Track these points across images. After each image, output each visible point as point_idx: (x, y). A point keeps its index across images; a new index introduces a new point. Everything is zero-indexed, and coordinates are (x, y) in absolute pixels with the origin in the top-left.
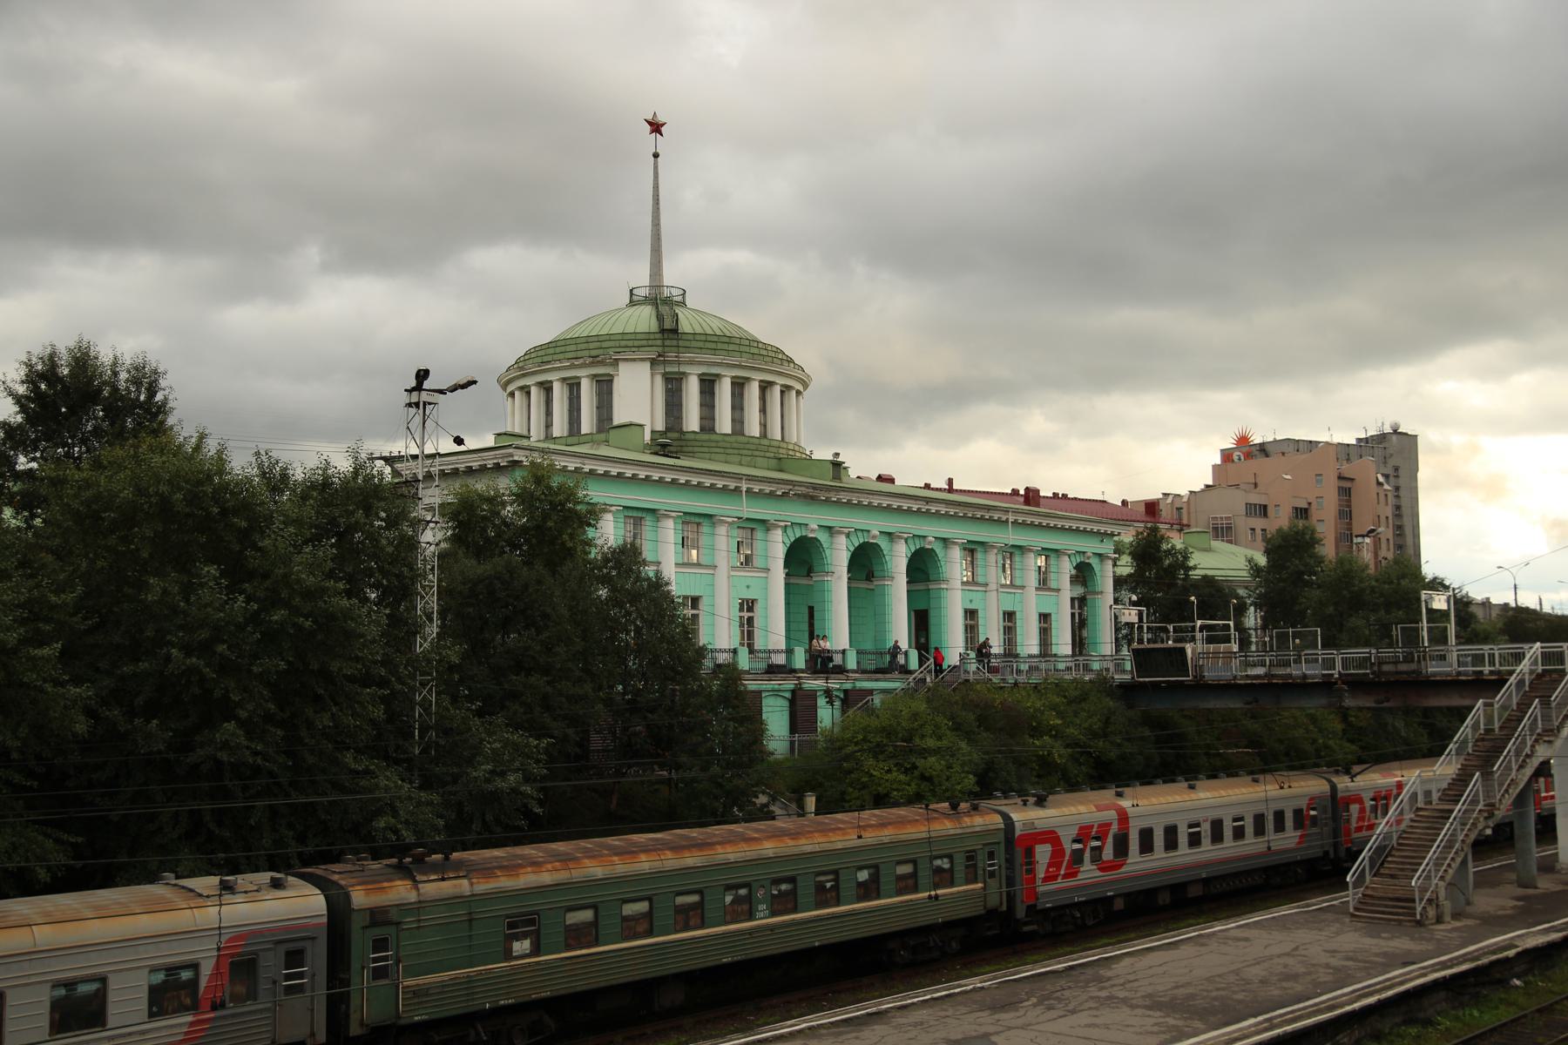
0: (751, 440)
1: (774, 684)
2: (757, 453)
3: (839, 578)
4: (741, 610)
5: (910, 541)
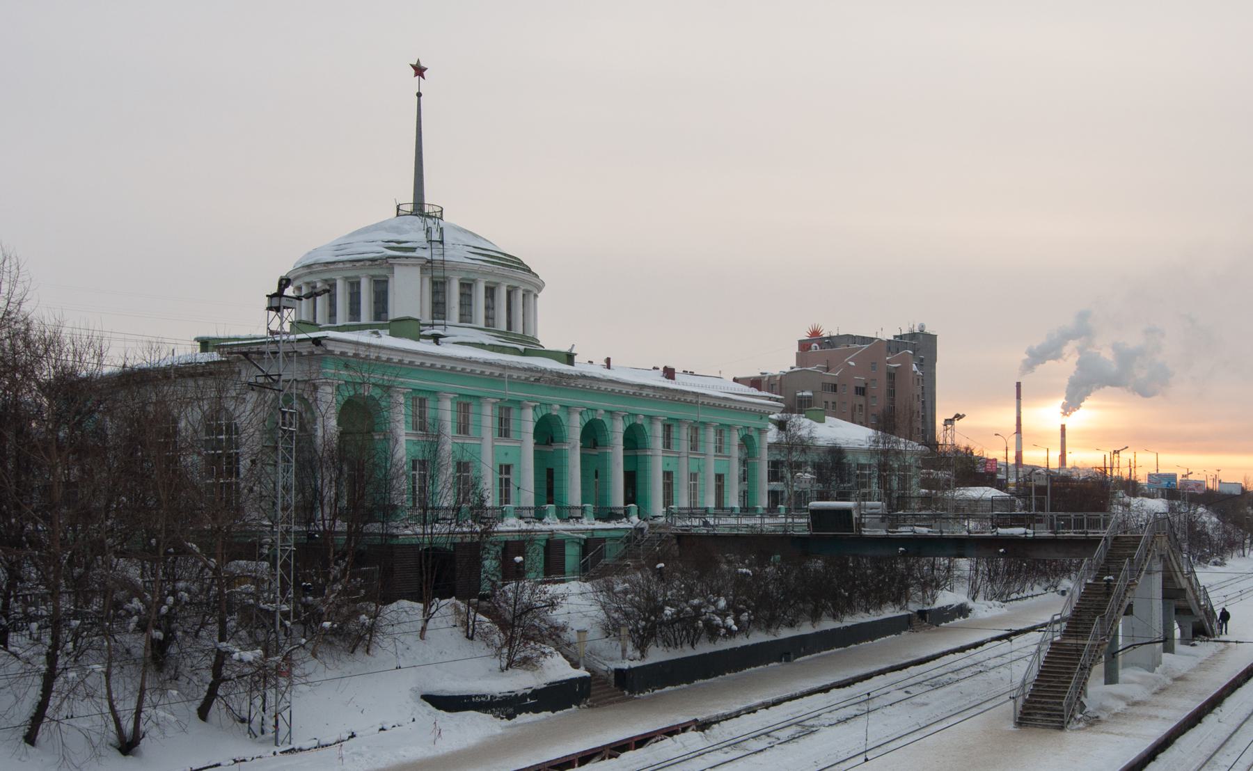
3: (574, 447)
4: (501, 473)
5: (626, 419)
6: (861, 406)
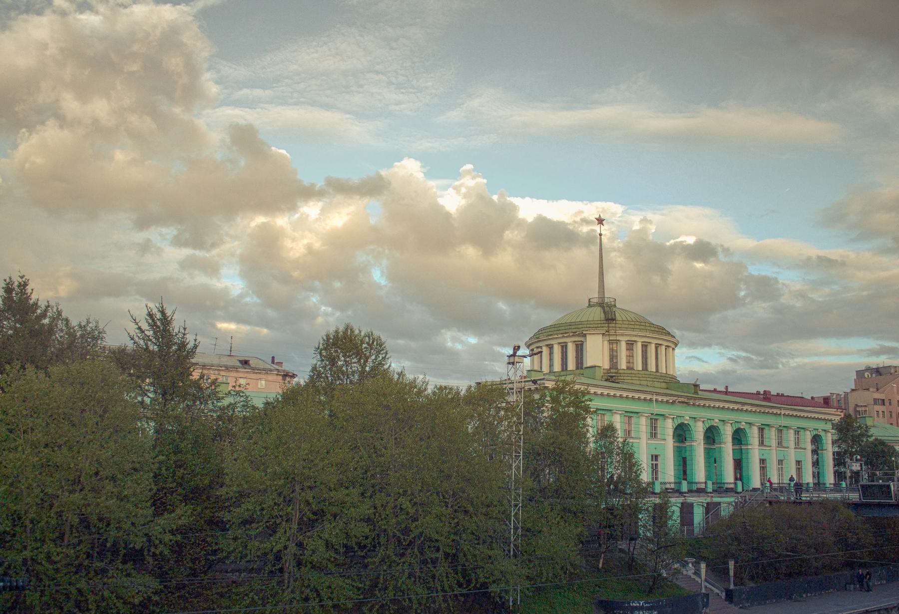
0: (652, 373)
2: (654, 380)
4: (652, 460)
5: (733, 425)
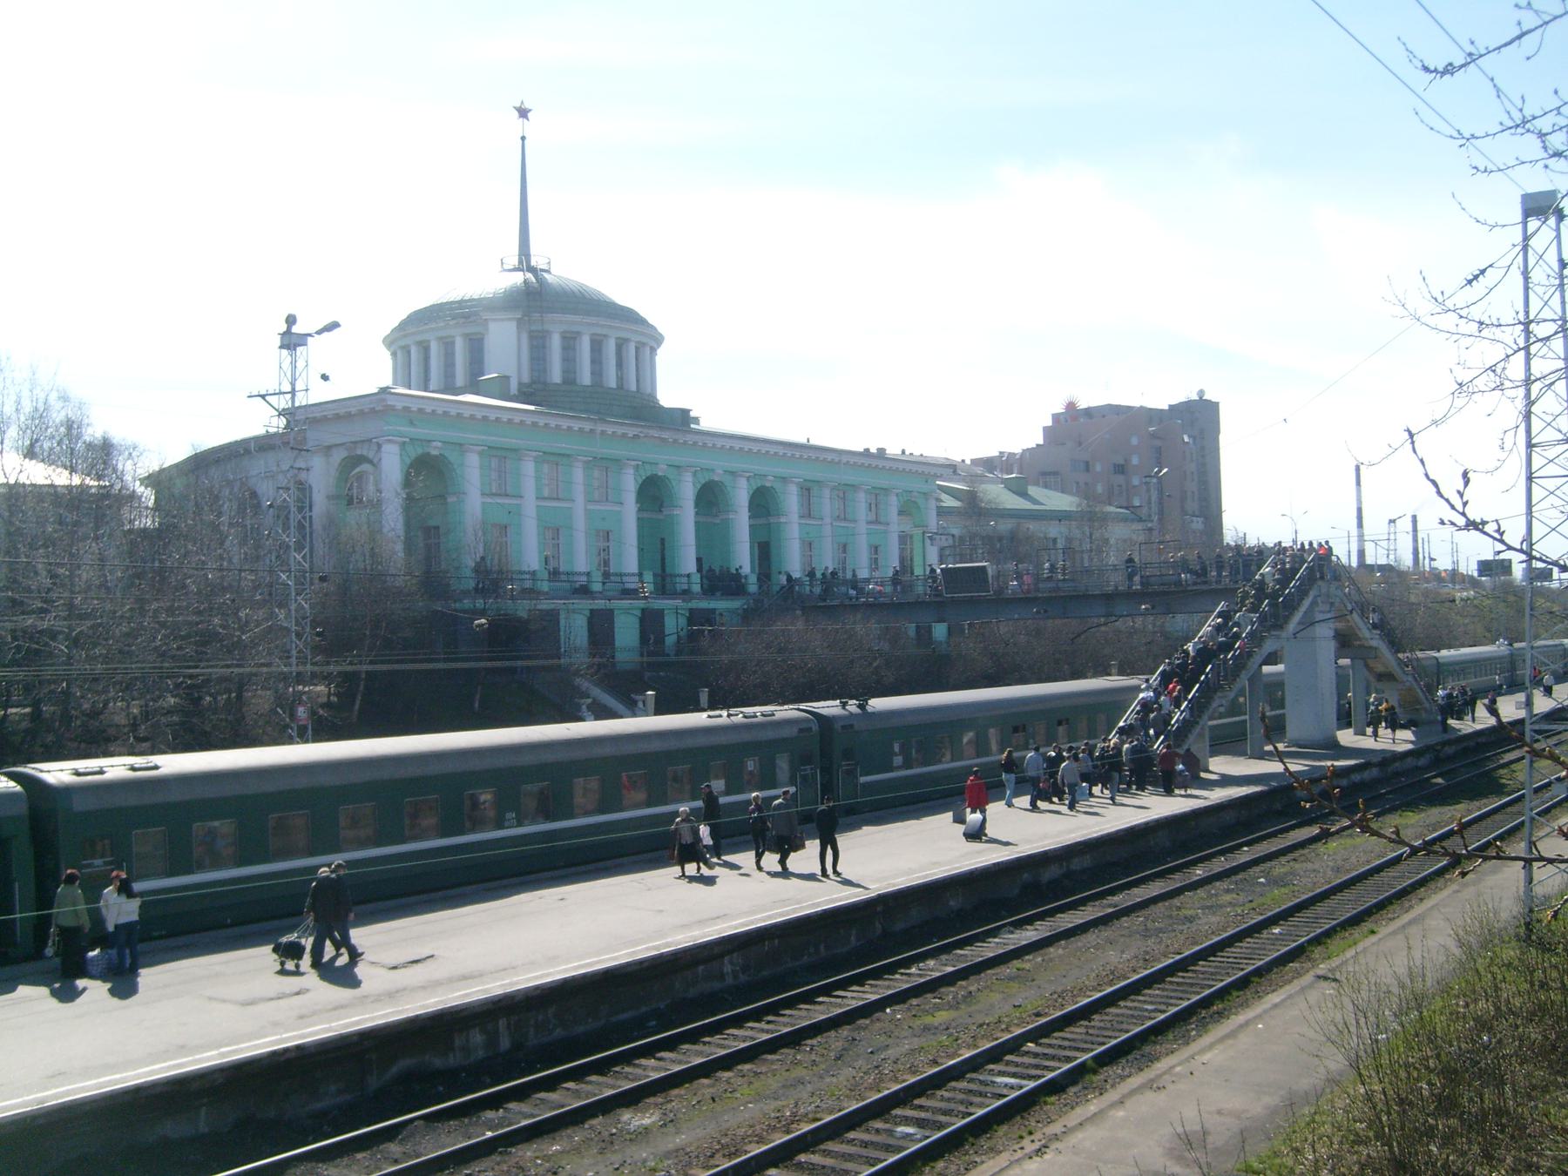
1: (626, 603)
6: (1120, 486)
